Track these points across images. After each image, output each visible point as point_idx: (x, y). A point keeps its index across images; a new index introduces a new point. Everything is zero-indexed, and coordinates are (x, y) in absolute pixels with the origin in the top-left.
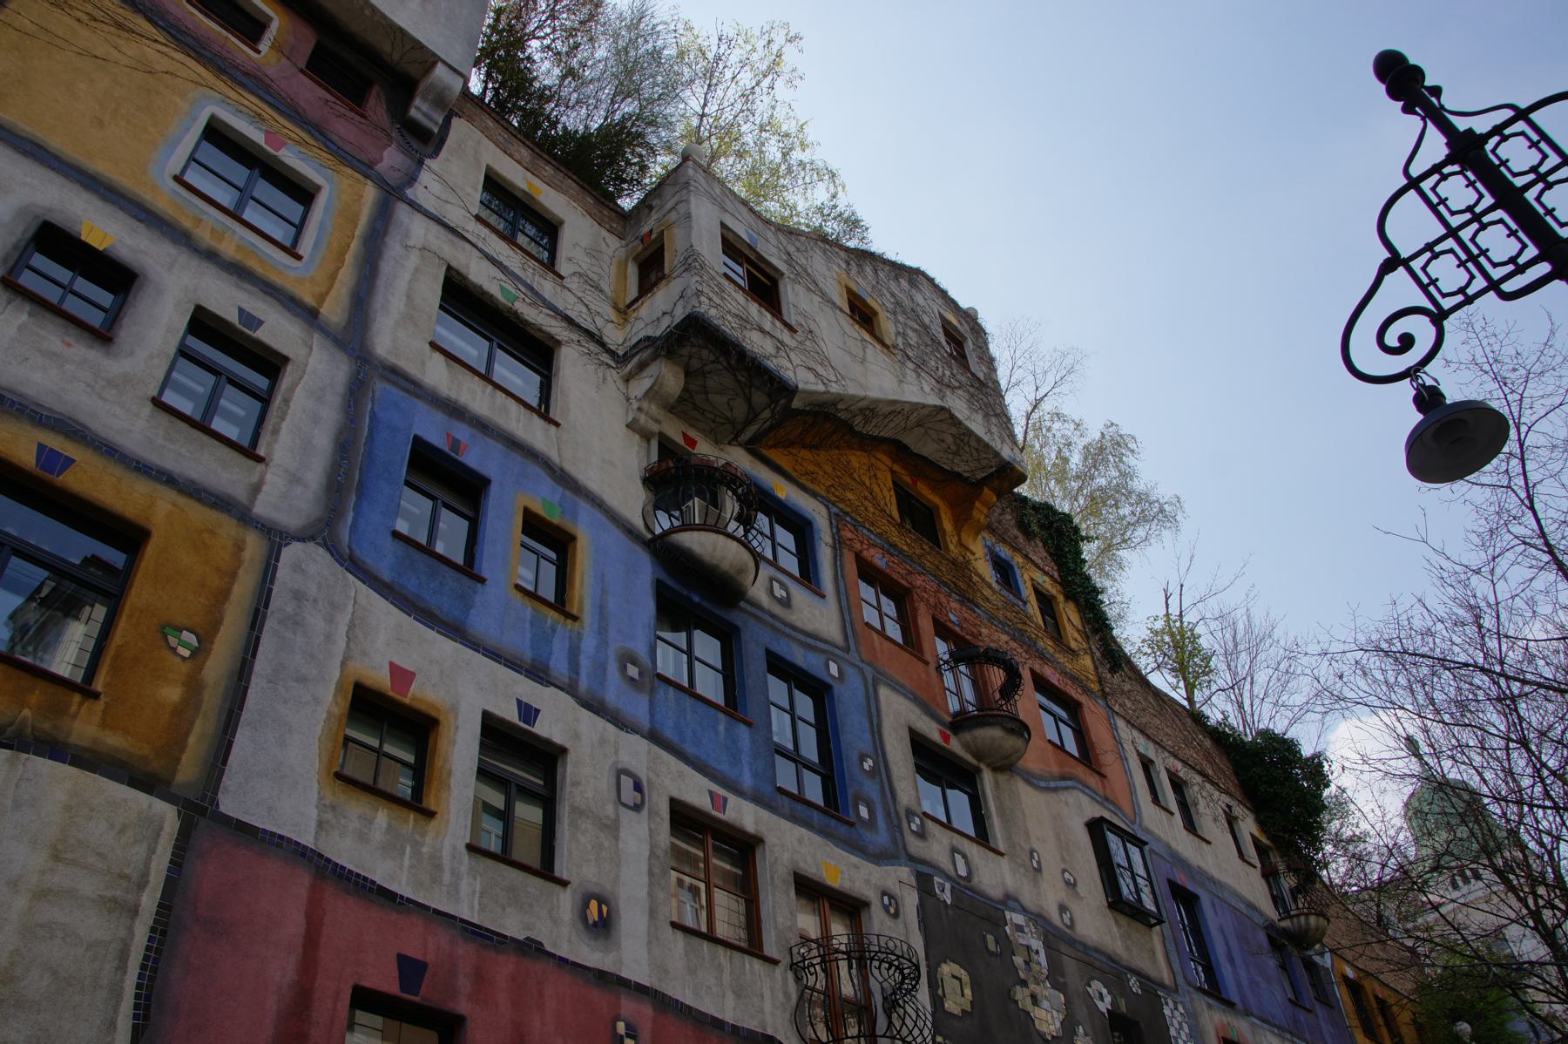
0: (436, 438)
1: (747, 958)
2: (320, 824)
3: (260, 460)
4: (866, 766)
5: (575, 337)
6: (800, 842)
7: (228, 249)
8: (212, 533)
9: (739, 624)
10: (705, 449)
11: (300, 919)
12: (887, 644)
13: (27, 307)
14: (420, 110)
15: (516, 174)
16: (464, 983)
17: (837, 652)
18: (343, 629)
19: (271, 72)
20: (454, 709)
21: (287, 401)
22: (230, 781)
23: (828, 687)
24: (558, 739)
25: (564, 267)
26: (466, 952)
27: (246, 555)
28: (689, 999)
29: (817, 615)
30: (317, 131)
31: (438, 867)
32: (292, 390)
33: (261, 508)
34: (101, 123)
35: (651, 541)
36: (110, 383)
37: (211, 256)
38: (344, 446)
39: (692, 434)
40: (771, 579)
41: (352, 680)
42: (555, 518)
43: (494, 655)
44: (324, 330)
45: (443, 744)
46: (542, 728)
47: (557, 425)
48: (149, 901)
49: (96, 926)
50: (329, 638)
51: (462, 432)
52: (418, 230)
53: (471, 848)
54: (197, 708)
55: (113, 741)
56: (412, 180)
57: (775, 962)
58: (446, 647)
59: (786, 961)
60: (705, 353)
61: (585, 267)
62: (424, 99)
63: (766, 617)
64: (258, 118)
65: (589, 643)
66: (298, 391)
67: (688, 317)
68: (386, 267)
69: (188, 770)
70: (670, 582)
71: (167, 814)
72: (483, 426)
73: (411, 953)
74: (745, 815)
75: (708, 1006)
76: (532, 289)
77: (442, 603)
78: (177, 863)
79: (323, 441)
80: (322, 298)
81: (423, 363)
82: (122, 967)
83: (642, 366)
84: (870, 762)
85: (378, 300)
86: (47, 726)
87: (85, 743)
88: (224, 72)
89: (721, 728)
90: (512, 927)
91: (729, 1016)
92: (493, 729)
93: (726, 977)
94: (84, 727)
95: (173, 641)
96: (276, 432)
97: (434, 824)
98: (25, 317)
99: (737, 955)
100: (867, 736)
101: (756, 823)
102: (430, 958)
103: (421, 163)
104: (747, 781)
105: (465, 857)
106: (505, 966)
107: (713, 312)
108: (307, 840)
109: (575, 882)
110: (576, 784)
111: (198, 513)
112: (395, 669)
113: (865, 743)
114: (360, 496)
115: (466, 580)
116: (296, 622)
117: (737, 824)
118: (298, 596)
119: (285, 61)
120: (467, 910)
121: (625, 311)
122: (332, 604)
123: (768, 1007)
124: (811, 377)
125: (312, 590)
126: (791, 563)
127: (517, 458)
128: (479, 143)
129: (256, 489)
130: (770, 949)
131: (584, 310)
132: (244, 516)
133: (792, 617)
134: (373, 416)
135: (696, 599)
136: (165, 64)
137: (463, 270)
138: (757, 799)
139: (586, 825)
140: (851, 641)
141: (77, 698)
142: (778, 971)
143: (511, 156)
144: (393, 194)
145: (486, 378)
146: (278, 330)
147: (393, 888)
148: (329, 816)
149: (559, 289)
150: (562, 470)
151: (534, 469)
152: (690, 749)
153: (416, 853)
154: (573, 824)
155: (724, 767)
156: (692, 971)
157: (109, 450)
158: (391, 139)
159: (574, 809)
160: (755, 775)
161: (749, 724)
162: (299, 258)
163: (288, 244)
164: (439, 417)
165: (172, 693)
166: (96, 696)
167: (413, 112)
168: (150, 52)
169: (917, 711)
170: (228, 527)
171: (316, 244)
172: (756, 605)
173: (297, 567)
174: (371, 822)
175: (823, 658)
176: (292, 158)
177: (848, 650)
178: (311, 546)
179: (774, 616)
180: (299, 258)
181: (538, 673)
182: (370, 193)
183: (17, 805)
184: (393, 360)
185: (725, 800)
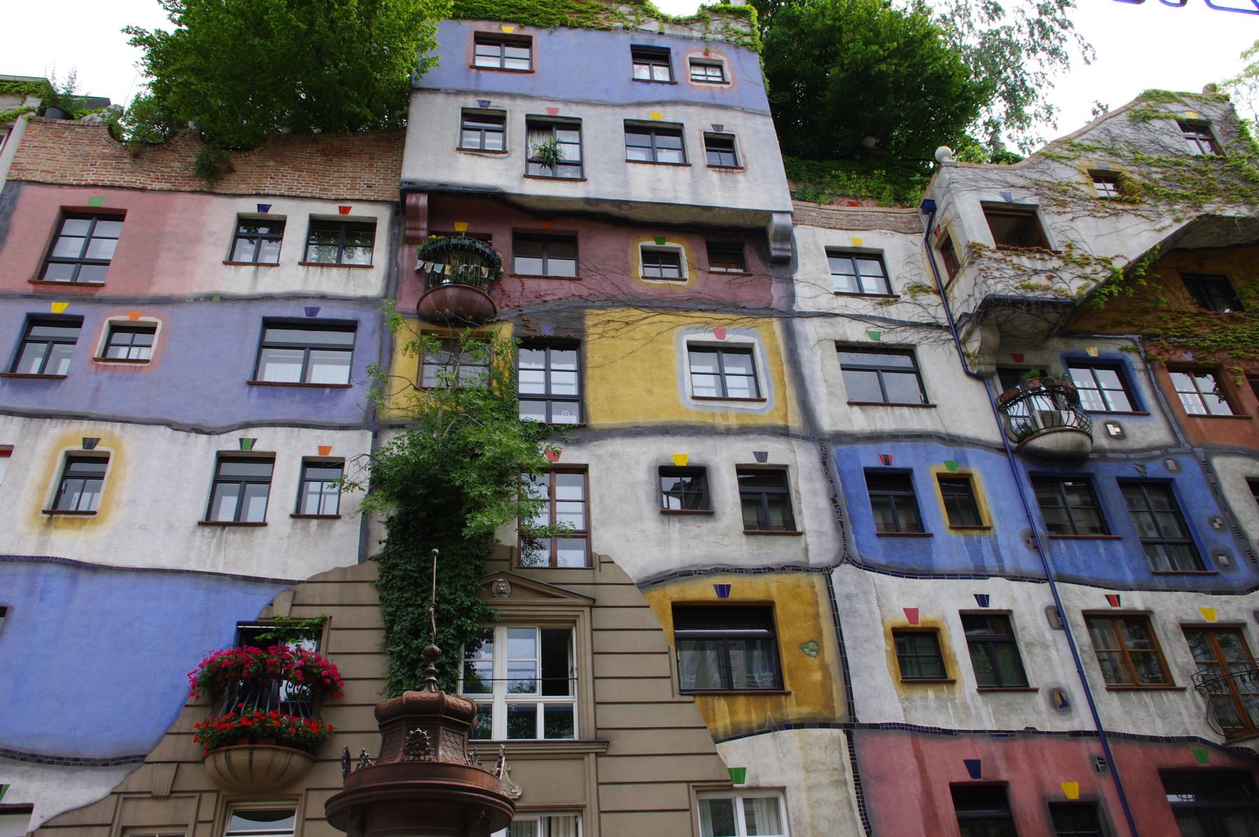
0: (876, 463)
1: (1163, 694)
2: (904, 710)
3: (800, 534)
4: (1216, 525)
5: (922, 335)
6: (1179, 602)
7: (733, 422)
8: (799, 586)
9: (1092, 471)
10: (1032, 358)
11: (914, 760)
12: (1209, 421)
13: (676, 518)
14: (776, 249)
15: (842, 239)
16: (1001, 764)
17: (1174, 450)
18: (875, 602)
19: (697, 287)
20: (944, 618)
21: (797, 492)
22: (858, 707)
23: (1172, 480)
24: (1004, 607)
25: (898, 288)
26: (996, 748)
27: (817, 589)
28: (1132, 731)
29: (1151, 432)
30: (736, 308)
31: (967, 708)
32: (797, 483)
33: (813, 560)
34: (650, 391)
35: (1018, 448)
36: (725, 535)
37: (728, 432)
38: (834, 500)
39: (1017, 352)
40: (1106, 424)
41: (889, 628)
42: (957, 470)
43: (953, 576)
44: (796, 437)
45: (946, 641)
46: (994, 605)
47: (935, 406)
48: (849, 776)
49: (834, 795)
50: (871, 612)
51: (886, 448)
52: (810, 330)
53: (981, 690)
54: (830, 677)
55: (805, 710)
56: (792, 297)
57: (1183, 690)
58: (927, 584)
59: (1190, 686)
60: (1005, 312)
61: (908, 275)
62: (775, 241)
63: (1110, 455)
64: (706, 326)
65: (1002, 540)
66: (801, 482)
67: (985, 301)
68: (806, 370)
69: (840, 711)
70: (1038, 469)
71: (839, 733)
72: (895, 437)
73: (971, 757)
74: (1134, 600)
75: (1146, 731)
76: (884, 320)
77: (916, 562)
78: (853, 757)
79: (824, 503)
80: (785, 417)
81: (850, 419)
82: (851, 809)
83: (969, 334)
84: (1219, 521)
85: (812, 394)
86: (778, 716)
87: (796, 716)
88: (678, 309)
89: (1102, 550)
90: (1016, 725)
91: (1161, 732)
92: (969, 619)
93: (1152, 710)
94: (793, 710)
95: (807, 651)
96: (800, 512)
97: (957, 685)
98: (678, 525)
99: (1155, 694)
100: (1212, 502)
101: (1144, 603)
102: (979, 757)
103: (792, 280)
104: (1129, 577)
105: (978, 697)
106: (1018, 747)
107: (1000, 287)
108: (902, 720)
109: (1041, 686)
110: (1023, 629)
111: (788, 579)
112: (907, 611)
113: (1212, 509)
114: (852, 522)
115: (923, 540)
116: (853, 612)
117: (1131, 608)
118: (848, 597)
119: (699, 273)
120: (990, 725)
121: (942, 292)
122: (865, 593)
123: (1186, 719)
124: (1081, 282)
125: (853, 590)
126: (1119, 402)
127: (921, 444)
128: (814, 235)
129: (806, 550)
130: (1179, 683)
131: (920, 309)
132: (809, 570)
133: (1130, 444)
134: (839, 469)
135: (1058, 471)
136: (653, 330)
137: (844, 339)
138: (1140, 588)
139: (1037, 650)
140: (1180, 437)
141: (783, 697)
142: (1188, 695)
143: (835, 228)
144: (788, 316)
145: (886, 404)
146: (777, 452)
147: (949, 727)
148: (907, 704)
149: (899, 306)
150: (948, 435)
151: (935, 445)
152: (1085, 575)
153: (954, 705)
154: (1030, 653)
155: (1111, 575)
156: (1128, 713)
157: (740, 571)
158: (770, 277)
159: (1027, 644)
160: (1134, 571)
161: (1119, 539)
162: (765, 400)
163: (755, 397)
164: (871, 447)
165: (817, 676)
166: (789, 693)
167: (774, 253)
168: (644, 327)
169: (1250, 461)
170: (802, 577)
171: (768, 383)
172: (1102, 453)
173: (842, 582)
174: (926, 698)
175: (1160, 462)
176: (732, 338)
177: (1178, 444)
178: (843, 566)
179: (1114, 451)
180: (765, 400)
181: (980, 574)
182: (777, 325)
183: (784, 755)
184: (835, 429)
185: (1118, 596)
